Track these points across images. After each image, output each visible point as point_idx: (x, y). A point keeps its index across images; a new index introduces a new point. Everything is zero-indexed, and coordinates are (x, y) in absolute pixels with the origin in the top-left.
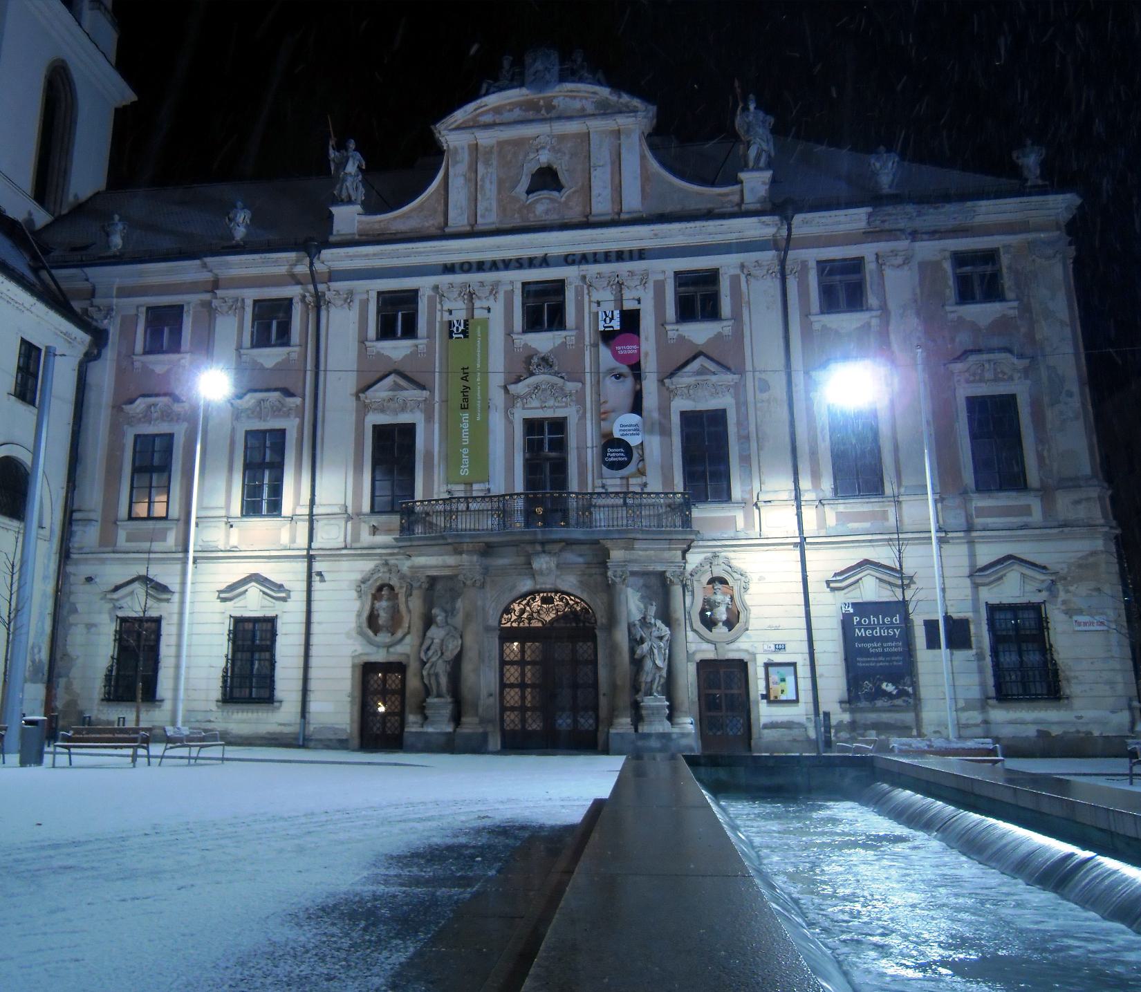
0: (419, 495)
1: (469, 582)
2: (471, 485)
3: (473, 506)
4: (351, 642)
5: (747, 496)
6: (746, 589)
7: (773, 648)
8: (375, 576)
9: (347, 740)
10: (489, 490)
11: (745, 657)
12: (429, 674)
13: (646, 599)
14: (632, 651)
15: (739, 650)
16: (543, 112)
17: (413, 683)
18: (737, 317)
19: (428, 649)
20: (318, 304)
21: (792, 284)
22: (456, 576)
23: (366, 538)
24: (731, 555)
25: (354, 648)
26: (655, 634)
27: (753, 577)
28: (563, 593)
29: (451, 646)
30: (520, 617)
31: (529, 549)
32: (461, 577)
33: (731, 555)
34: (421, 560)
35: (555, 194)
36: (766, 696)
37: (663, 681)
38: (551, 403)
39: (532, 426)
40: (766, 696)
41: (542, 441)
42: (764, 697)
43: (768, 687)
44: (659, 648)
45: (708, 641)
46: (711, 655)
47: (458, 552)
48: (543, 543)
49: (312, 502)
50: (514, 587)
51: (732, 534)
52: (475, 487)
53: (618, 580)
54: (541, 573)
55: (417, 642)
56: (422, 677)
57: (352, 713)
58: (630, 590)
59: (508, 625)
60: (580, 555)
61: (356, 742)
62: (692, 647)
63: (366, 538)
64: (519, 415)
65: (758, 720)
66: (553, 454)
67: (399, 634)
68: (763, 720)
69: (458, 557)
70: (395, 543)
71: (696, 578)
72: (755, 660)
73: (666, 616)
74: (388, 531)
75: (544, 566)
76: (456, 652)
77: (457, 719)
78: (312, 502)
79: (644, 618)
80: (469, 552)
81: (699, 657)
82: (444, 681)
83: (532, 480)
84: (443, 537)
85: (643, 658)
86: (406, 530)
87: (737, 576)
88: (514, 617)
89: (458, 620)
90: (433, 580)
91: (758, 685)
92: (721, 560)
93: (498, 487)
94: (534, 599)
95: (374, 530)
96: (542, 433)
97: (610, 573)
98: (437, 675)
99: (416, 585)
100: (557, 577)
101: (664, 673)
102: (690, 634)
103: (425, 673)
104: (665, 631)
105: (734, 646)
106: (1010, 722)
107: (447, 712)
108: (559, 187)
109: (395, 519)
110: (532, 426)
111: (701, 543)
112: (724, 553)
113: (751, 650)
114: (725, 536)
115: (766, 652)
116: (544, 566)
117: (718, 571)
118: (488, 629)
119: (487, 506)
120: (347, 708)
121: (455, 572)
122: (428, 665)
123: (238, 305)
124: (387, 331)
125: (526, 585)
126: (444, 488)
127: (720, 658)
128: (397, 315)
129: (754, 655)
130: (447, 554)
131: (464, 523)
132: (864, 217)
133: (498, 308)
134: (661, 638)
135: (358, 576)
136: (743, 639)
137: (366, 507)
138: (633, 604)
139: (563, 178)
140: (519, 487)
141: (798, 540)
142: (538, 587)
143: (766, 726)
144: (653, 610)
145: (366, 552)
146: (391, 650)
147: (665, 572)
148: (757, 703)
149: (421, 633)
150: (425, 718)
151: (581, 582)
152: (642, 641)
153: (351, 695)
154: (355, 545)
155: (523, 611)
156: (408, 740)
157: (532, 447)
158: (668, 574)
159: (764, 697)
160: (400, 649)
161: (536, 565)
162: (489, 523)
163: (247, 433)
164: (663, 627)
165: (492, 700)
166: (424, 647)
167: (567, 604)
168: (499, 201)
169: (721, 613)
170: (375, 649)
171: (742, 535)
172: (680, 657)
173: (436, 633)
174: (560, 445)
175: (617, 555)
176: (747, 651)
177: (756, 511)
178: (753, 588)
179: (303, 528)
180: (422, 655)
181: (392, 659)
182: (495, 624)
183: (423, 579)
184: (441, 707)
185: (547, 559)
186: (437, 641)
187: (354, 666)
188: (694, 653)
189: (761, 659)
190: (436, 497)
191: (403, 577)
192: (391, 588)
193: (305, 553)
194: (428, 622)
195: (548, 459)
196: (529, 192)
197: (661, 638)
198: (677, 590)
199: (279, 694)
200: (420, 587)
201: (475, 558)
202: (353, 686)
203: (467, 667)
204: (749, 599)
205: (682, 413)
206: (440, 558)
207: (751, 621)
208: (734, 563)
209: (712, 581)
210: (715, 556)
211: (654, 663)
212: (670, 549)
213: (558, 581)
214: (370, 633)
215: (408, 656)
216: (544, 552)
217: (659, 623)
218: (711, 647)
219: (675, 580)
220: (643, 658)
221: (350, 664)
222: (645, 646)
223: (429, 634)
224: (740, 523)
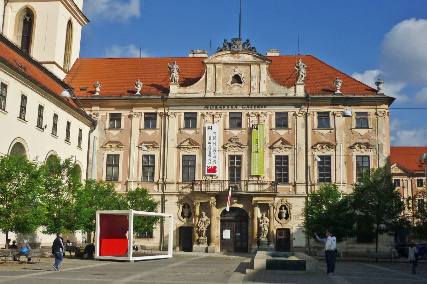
6: (291, 208)
13: (262, 211)
14: (258, 226)
15: (288, 226)
16: (237, 58)
18: (293, 129)
20: (165, 116)
21: (309, 119)
27: (293, 205)
29: (207, 223)
35: (239, 84)
38: (237, 150)
39: (231, 157)
41: (234, 162)
49: (163, 179)
64: (228, 154)
65: (292, 245)
66: (237, 166)
67: (191, 218)
71: (277, 205)
72: (292, 228)
76: (208, 225)
77: (209, 242)
78: (163, 179)
81: (277, 228)
83: (231, 175)
85: (261, 227)
87: (289, 205)
96: (234, 160)
106: (360, 248)
108: (241, 83)
110: (231, 157)
114: (286, 193)
123: (139, 115)
124: (187, 127)
128: (190, 120)
132: (330, 101)
133: (222, 120)
134: (266, 222)
137: (181, 181)
139: (243, 79)
141: (306, 195)
144: (265, 214)
152: (261, 223)
157: (231, 163)
158: (269, 204)
163: (143, 155)
164: (267, 219)
165: (218, 238)
168: (223, 86)
169: (284, 215)
172: (272, 228)
174: (239, 163)
178: (293, 208)
179: (160, 186)
181: (188, 226)
192: (188, 205)
193: (162, 193)
195: (236, 167)
196: (232, 83)
197: (266, 222)
199: (154, 235)
202: (177, 233)
204: (291, 211)
205: (276, 156)
208: (289, 201)
214: (182, 218)
217: (266, 218)
218: (280, 224)
222: (262, 225)
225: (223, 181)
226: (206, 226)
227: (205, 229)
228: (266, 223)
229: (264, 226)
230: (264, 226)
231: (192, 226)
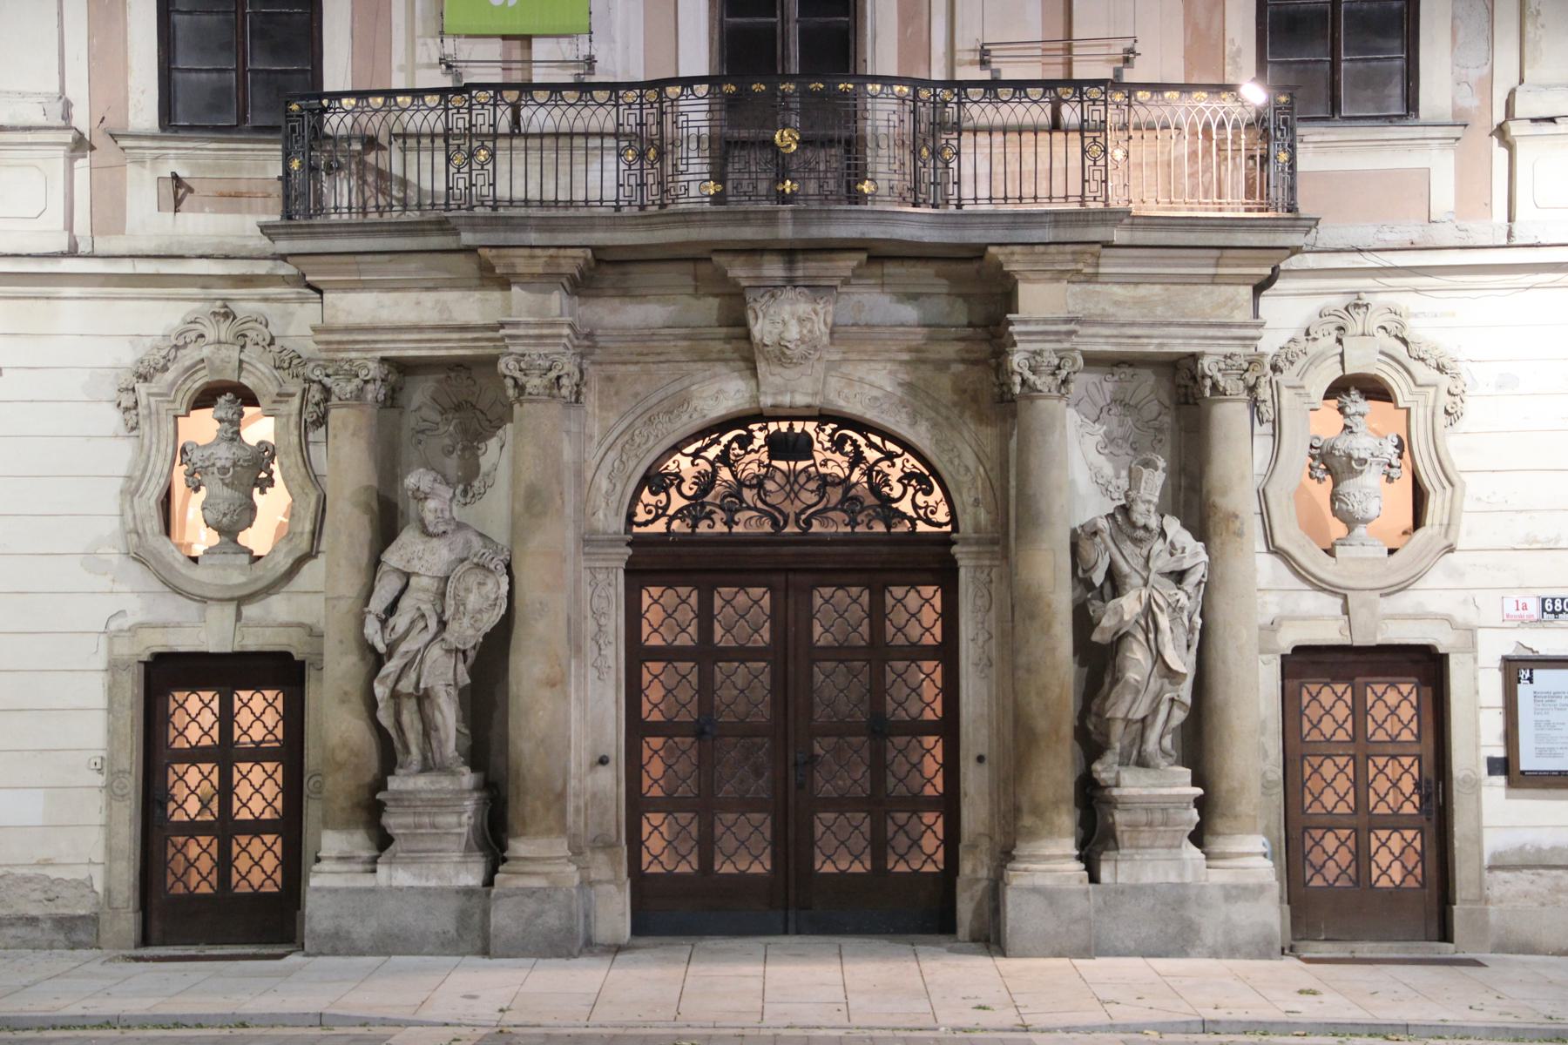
0: (337, 75)
1: (534, 383)
2: (526, 39)
3: (538, 117)
4: (103, 583)
5: (1470, 102)
7: (1534, 609)
8: (190, 355)
9: (93, 920)
10: (590, 61)
11: (1442, 639)
12: (395, 695)
13: (1131, 448)
14: (1083, 621)
17: (336, 724)
19: (392, 609)
22: (493, 361)
23: (147, 220)
24: (1405, 302)
25: (110, 606)
26: (1162, 562)
28: (846, 421)
29: (473, 601)
30: (697, 500)
31: (739, 271)
32: (507, 366)
33: (1405, 302)
34: (355, 306)
36: (1505, 766)
37: (1179, 716)
40: (1505, 766)
42: (1495, 766)
43: (1511, 735)
44: (1176, 609)
45: (1320, 586)
46: (1330, 633)
47: (493, 278)
48: (790, 253)
50: (681, 401)
51: (1414, 233)
52: (540, 49)
53: (1042, 382)
54: (781, 355)
55: (349, 585)
56: (371, 704)
57: (108, 826)
58: (1072, 417)
59: (659, 527)
60: (913, 297)
61: (127, 922)
62: (1269, 606)
63: (147, 220)
68: (1493, 842)
69: (496, 295)
70: (263, 243)
71: (1288, 376)
72: (1471, 647)
73: (1193, 502)
74: (232, 198)
75: (793, 332)
76: (491, 619)
77: (493, 838)
79: (1125, 510)
80: (533, 281)
82: (448, 715)
84: (442, 226)
85: (1120, 639)
86: (298, 205)
87: (1423, 372)
88: (678, 502)
89: (495, 509)
90: (402, 369)
91: (1476, 731)
92: (1374, 320)
93: (622, 60)
94: (745, 441)
95: (179, 191)
97: (1018, 360)
98: (423, 698)
99: (343, 388)
100: (832, 366)
101: (1185, 692)
102: (1266, 567)
103: (381, 691)
104: (1193, 553)
105: (1404, 602)
107: (464, 818)
109: (264, 163)
111: (1310, 261)
112: (1385, 297)
113: (1462, 615)
114: (1393, 238)
115: (1507, 623)
116: (793, 332)
117: (1362, 360)
118: (590, 541)
119: (601, 118)
120: (93, 809)
121: (487, 349)
122: (391, 667)
125: (726, 393)
126: (430, 50)
127: (1359, 641)
129: (1471, 630)
130: (453, 285)
131: (515, 178)
134: (1179, 577)
135: (128, 356)
136: (1435, 578)
138: (1083, 465)
140: (696, 57)
142: (767, 401)
143: (1500, 865)
144: (1154, 483)
145: (151, 275)
146: (250, 611)
147: (1195, 357)
148: (1476, 786)
149: (364, 557)
150: (383, 841)
151: (909, 387)
152: (1115, 583)
153: (107, 766)
154: (102, 246)
155: (706, 482)
156: (317, 912)
158: (1207, 364)
159: (1495, 766)
160: (279, 607)
161: (762, 329)
162: (601, 178)
166: (378, 603)
167: (857, 458)
170: (193, 607)
171: (1446, 235)
173: (407, 550)
175: (1039, 300)
176: (1448, 619)
177: (1501, 154)
178: (1474, 411)
180: (372, 629)
181: (252, 641)
182: (618, 524)
183: (374, 370)
184: (439, 795)
185: (804, 308)
186: (423, 584)
187: (114, 667)
188: (1274, 626)
189: (1495, 646)
190: (398, 82)
191: (289, 363)
194: (387, 520)
198: (1231, 417)
200: (359, 394)
201: (556, 301)
202: (112, 732)
203: (527, 669)
204: (1459, 447)
206: (429, 298)
207: (1466, 522)
209: (1337, 390)
210: (1357, 305)
211: (1158, 657)
212: (1214, 280)
213: (834, 382)
215: (314, 634)
216: (791, 282)
217: (1173, 526)
219: (1230, 384)
220: (1120, 639)
221: (101, 663)
223: (393, 557)
224: (1443, 196)
225: (660, 85)
226: (468, 631)
227: (442, 675)
228: (1168, 587)
229: (1149, 612)
230: (1149, 612)
231: (297, 646)
